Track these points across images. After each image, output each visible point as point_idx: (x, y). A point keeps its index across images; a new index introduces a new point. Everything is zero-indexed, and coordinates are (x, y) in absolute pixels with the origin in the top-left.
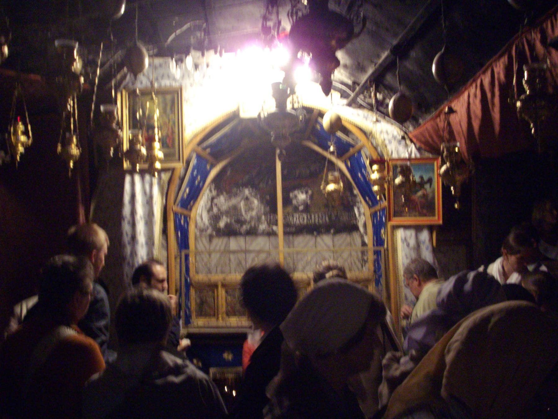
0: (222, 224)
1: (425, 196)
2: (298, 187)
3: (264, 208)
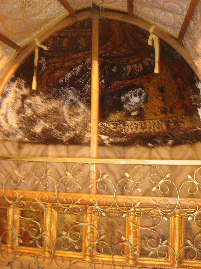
0: (38, 129)
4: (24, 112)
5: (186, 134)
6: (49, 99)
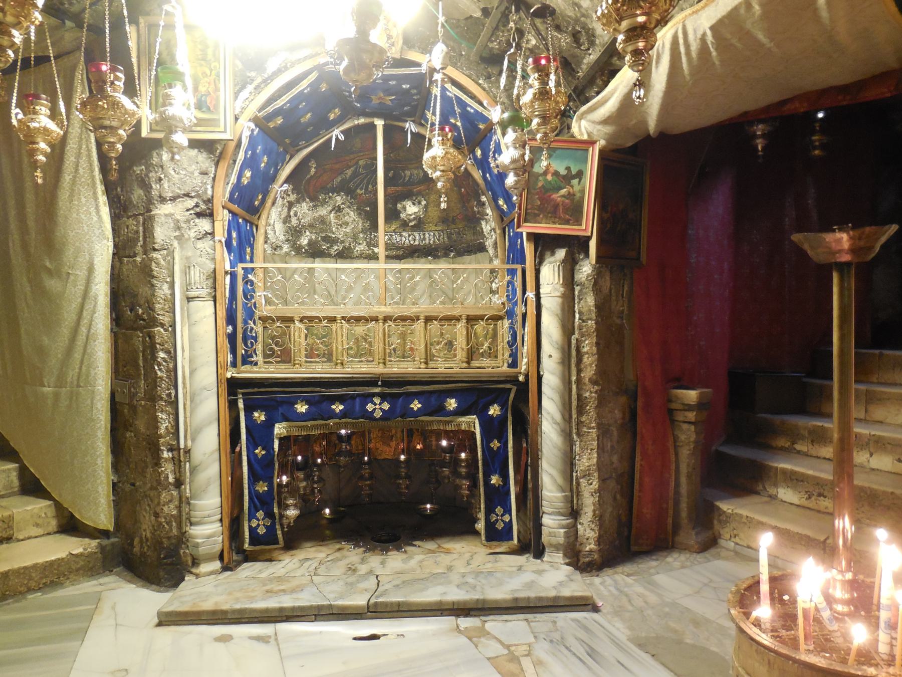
0: (304, 241)
1: (570, 195)
2: (408, 195)
5: (468, 246)
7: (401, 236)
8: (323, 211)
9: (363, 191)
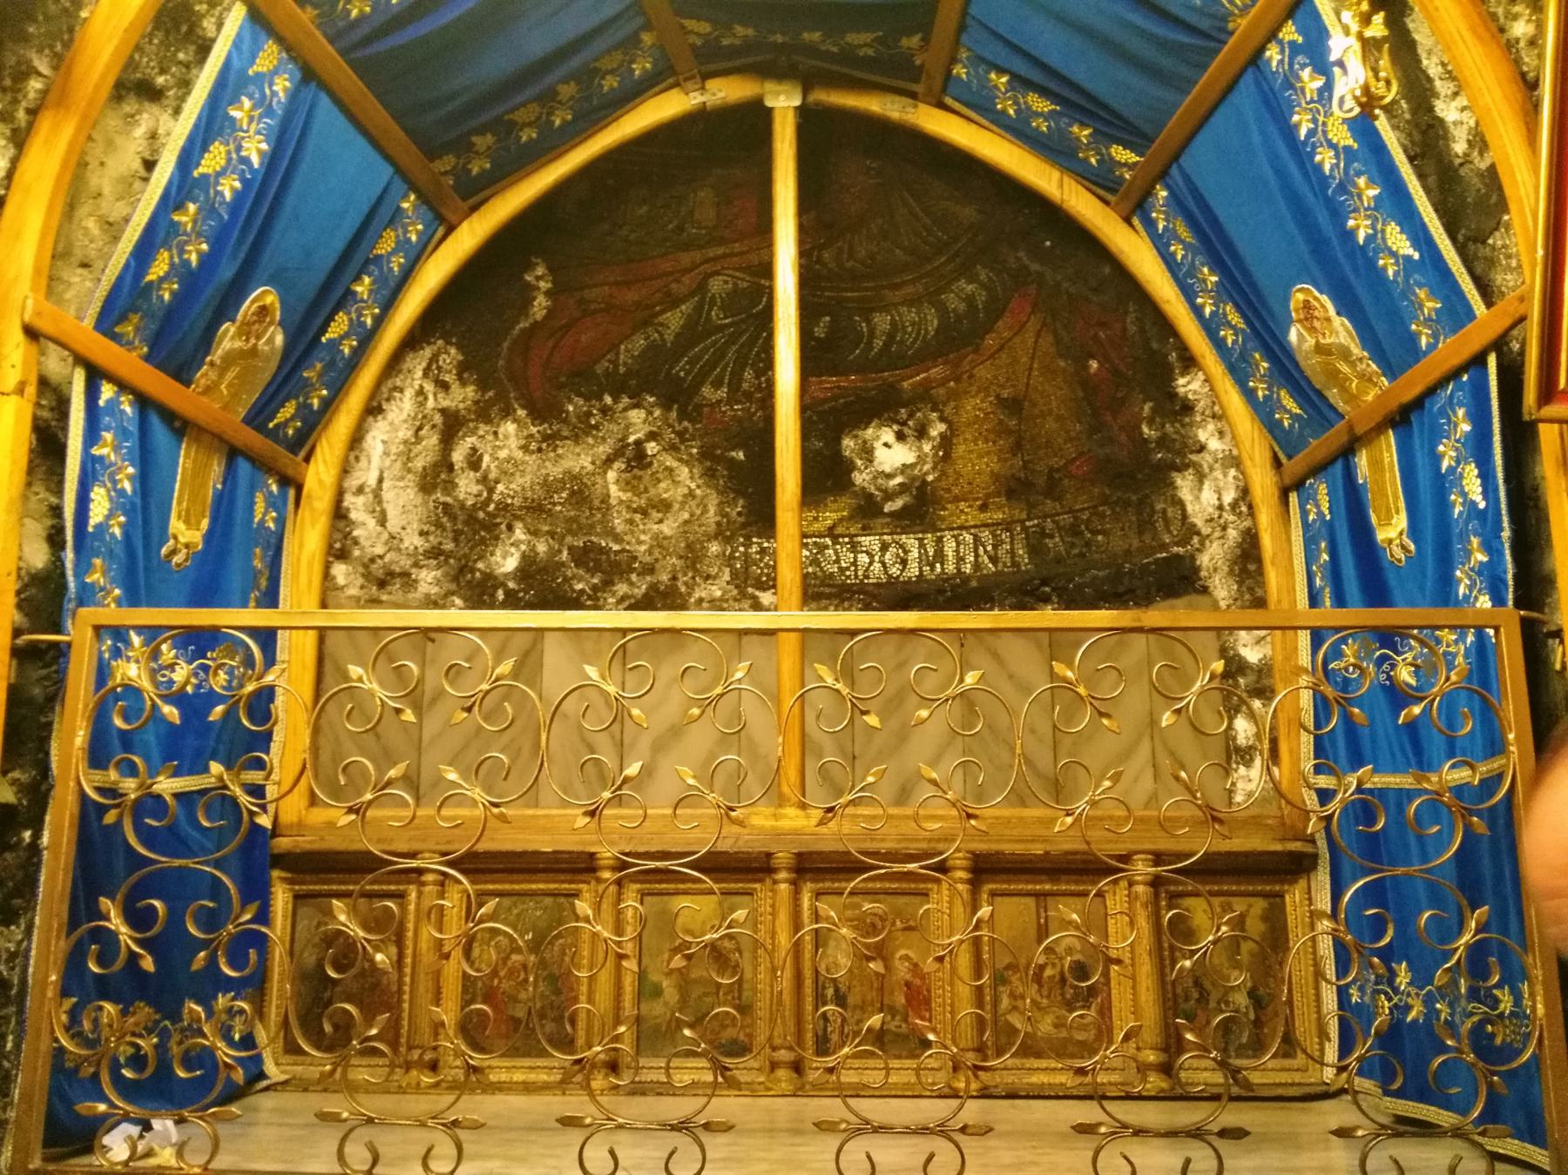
0: (507, 562)
2: (883, 406)
3: (721, 504)
4: (450, 486)
5: (1118, 575)
6: (550, 439)
7: (854, 548)
8: (578, 459)
9: (723, 393)
